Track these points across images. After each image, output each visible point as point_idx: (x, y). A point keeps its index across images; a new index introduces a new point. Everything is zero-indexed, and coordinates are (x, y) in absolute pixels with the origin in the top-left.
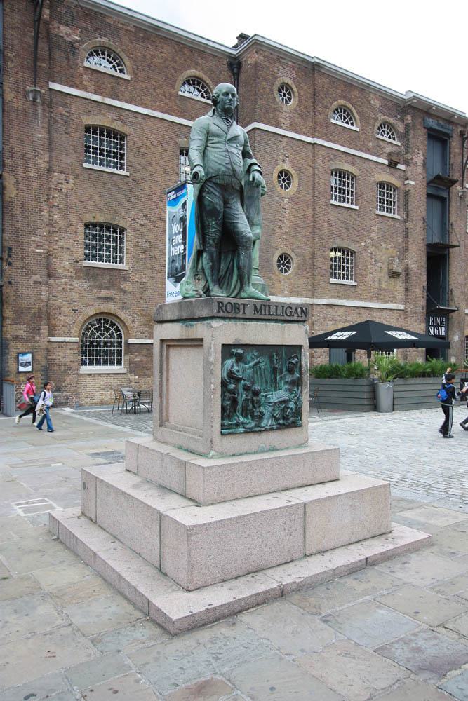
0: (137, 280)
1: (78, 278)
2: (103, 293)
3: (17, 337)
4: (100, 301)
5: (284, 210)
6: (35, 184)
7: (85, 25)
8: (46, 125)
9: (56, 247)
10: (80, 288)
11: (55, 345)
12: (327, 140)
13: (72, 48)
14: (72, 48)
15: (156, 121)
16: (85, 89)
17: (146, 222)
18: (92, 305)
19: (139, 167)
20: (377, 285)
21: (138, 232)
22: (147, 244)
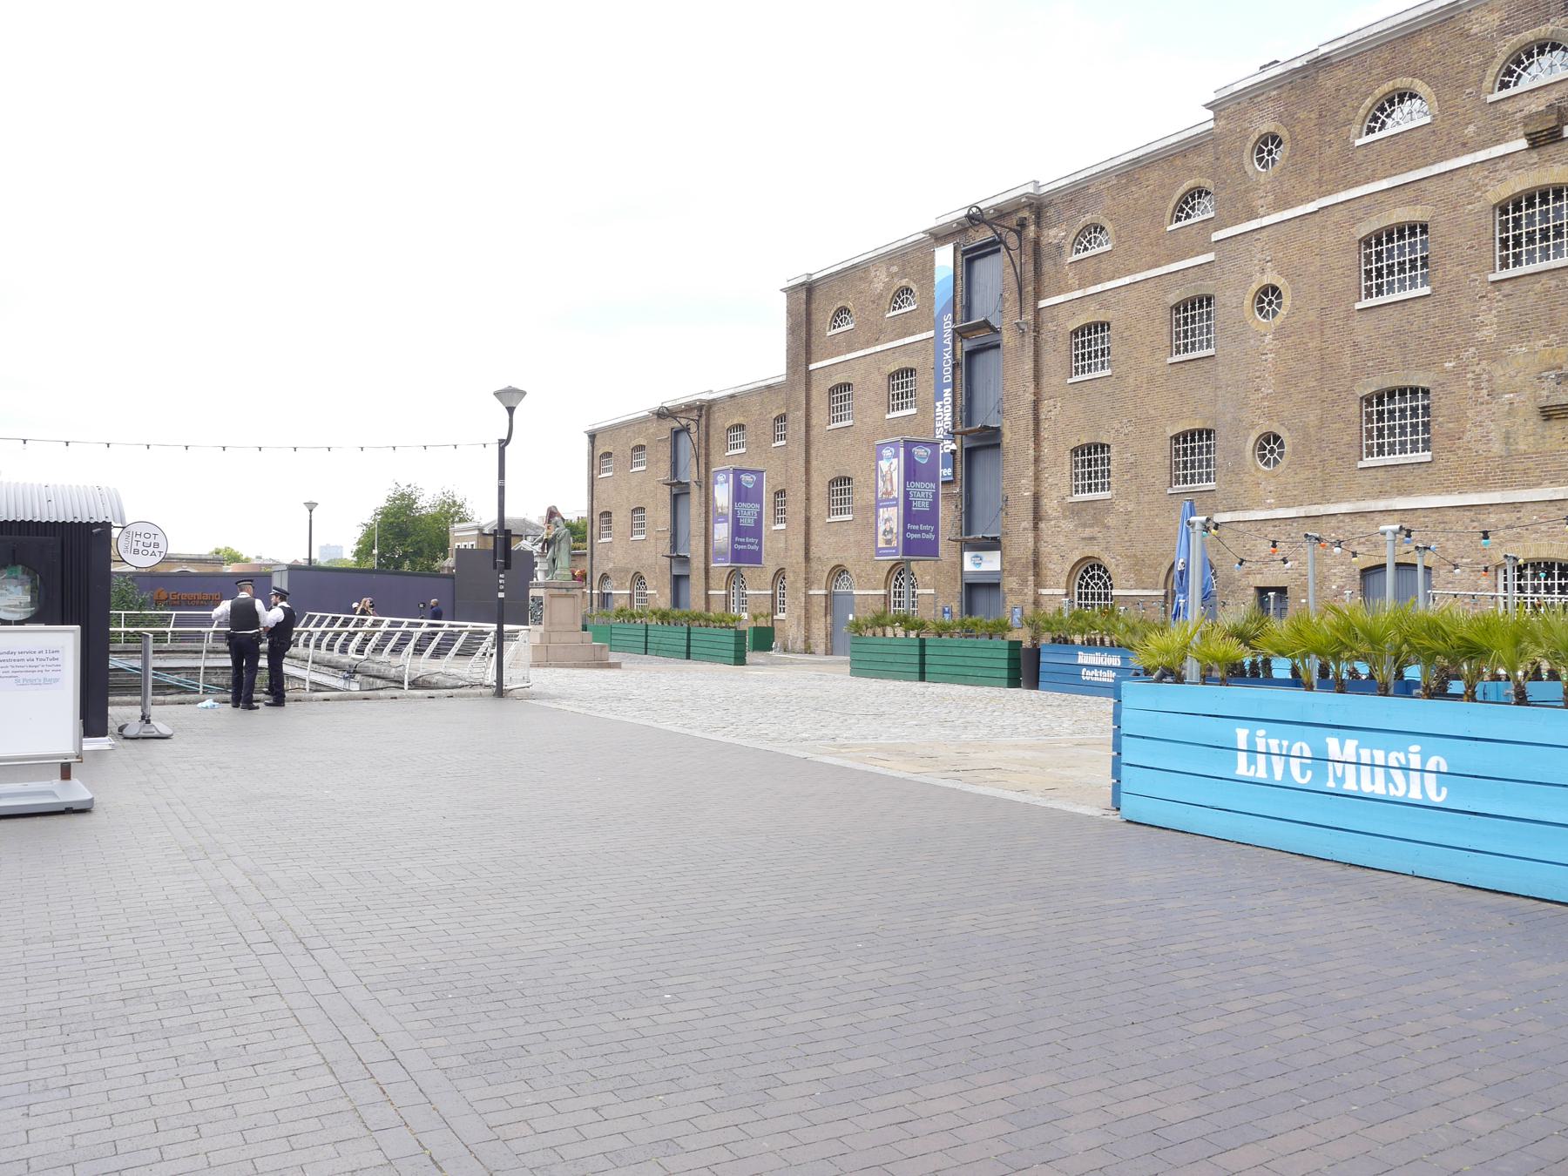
0: (1121, 510)
1: (1065, 517)
2: (1088, 532)
3: (1011, 590)
4: (1084, 543)
5: (1263, 357)
6: (1024, 422)
7: (1068, 214)
8: (1031, 354)
9: (1046, 485)
10: (1066, 530)
11: (1046, 599)
12: (1347, 188)
13: (1059, 247)
14: (1059, 247)
15: (1141, 285)
16: (1071, 289)
17: (1130, 428)
18: (1077, 548)
19: (1122, 358)
20: (1497, 448)
21: (1122, 446)
22: (1132, 460)
